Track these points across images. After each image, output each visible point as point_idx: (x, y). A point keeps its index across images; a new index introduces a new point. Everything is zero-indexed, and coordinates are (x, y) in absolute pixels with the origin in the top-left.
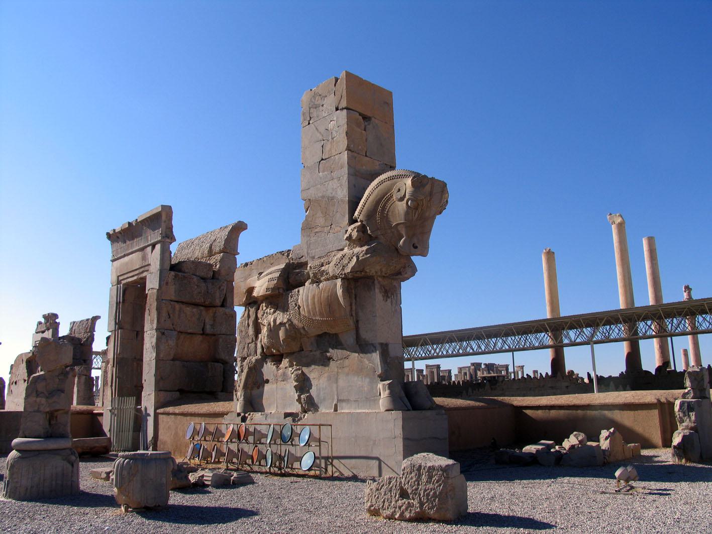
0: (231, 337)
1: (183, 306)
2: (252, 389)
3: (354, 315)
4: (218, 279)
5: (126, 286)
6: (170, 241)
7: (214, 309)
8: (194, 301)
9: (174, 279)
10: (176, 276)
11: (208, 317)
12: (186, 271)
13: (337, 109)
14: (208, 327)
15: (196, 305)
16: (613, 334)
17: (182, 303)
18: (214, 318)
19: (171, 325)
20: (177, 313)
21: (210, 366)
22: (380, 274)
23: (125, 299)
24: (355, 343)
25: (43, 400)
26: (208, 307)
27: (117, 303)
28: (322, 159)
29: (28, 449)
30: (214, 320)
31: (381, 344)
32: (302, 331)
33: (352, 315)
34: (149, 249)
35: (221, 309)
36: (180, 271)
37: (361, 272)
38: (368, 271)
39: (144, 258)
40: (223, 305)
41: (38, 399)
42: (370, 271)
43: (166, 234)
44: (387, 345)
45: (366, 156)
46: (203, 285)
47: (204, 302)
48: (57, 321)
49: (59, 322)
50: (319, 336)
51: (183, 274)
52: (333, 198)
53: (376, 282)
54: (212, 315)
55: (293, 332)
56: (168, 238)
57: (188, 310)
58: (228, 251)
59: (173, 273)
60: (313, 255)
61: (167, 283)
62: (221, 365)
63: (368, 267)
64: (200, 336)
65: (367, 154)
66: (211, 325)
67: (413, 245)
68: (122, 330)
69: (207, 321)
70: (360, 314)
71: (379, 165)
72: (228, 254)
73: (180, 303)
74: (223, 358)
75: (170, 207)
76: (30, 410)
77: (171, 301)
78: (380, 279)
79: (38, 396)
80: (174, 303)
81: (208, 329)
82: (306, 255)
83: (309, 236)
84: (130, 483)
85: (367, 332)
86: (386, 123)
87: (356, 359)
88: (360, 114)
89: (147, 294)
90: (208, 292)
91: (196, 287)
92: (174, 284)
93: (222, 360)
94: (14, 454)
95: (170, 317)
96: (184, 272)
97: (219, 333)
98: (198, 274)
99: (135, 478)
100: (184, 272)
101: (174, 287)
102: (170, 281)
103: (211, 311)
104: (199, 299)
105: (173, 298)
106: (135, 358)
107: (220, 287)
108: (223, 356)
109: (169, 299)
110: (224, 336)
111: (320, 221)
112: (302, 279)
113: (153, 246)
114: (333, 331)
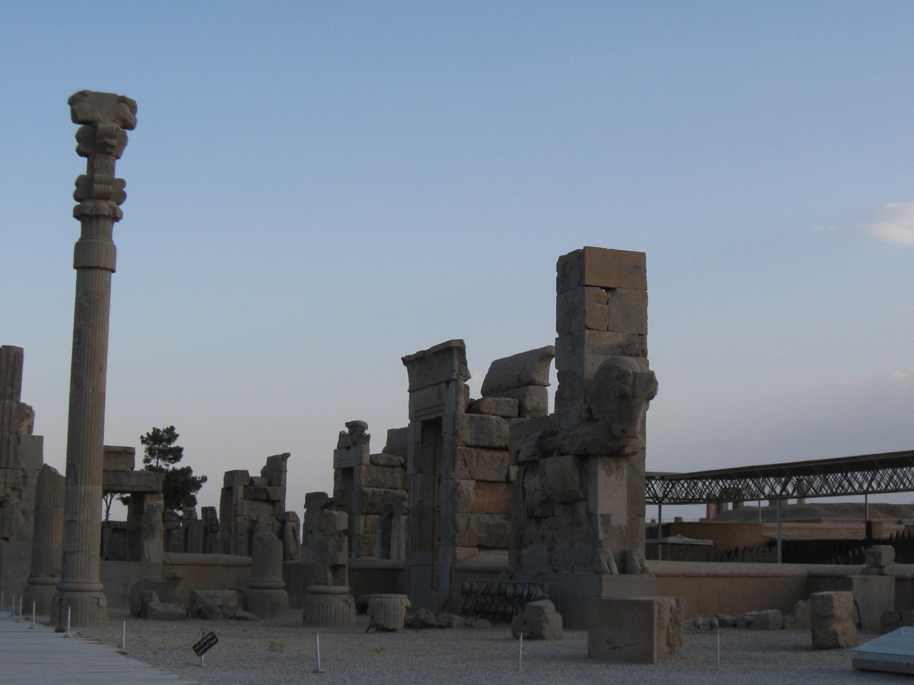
9: (469, 423)
10: (472, 419)
12: (485, 411)
27: (415, 443)
28: (570, 333)
34: (444, 385)
36: (478, 411)
44: (609, 516)
48: (367, 432)
49: (369, 435)
51: (479, 415)
65: (609, 329)
71: (624, 336)
80: (470, 449)
86: (636, 289)
92: (470, 428)
95: (466, 464)
96: (483, 413)
98: (499, 413)
100: (483, 413)
102: (465, 425)
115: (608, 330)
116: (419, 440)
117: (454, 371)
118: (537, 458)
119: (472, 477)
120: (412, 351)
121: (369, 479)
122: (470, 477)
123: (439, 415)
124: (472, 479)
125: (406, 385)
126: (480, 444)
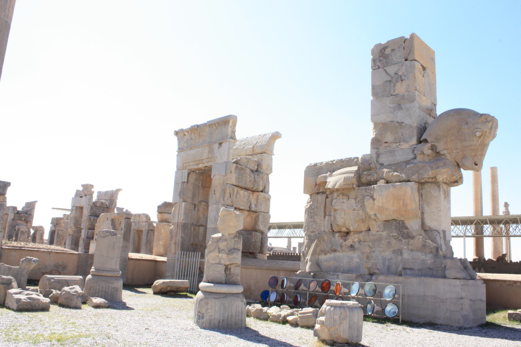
0: (267, 214)
1: (239, 189)
2: (319, 255)
3: (421, 208)
4: (260, 172)
5: (190, 171)
6: (233, 141)
7: (257, 193)
8: (247, 186)
10: (237, 167)
11: (253, 198)
12: (242, 164)
14: (253, 206)
15: (246, 189)
16: (487, 231)
17: (238, 187)
18: (257, 199)
19: (231, 203)
20: (235, 194)
21: (254, 235)
22: (445, 181)
23: (189, 180)
24: (421, 228)
25: (224, 256)
26: (253, 191)
29: (218, 292)
30: (257, 202)
31: (443, 231)
32: (373, 217)
33: (420, 209)
34: (216, 146)
35: (262, 194)
37: (432, 178)
38: (438, 178)
39: (211, 151)
40: (262, 191)
41: (220, 255)
42: (439, 178)
43: (231, 136)
45: (424, 96)
46: (252, 175)
47: (253, 188)
50: (386, 221)
52: (401, 123)
53: (441, 186)
54: (256, 197)
55: (364, 217)
56: (233, 139)
57: (242, 192)
58: (268, 152)
60: (382, 162)
61: (231, 172)
62: (260, 234)
63: (439, 176)
64: (247, 212)
66: (255, 205)
67: (475, 163)
68: (185, 203)
69: (252, 201)
70: (426, 208)
72: (268, 155)
73: (237, 187)
74: (261, 229)
75: (236, 117)
76: (213, 263)
77: (233, 185)
78: (443, 184)
79: (219, 252)
81: (253, 208)
82: (375, 162)
83: (377, 148)
84: (341, 325)
85: (431, 221)
87: (421, 240)
89: (212, 179)
90: (255, 181)
91: (248, 176)
93: (260, 230)
94: (200, 294)
97: (259, 211)
99: (344, 322)
100: (242, 165)
101: (235, 174)
102: (233, 170)
103: (255, 195)
104: (250, 186)
105: (234, 183)
106: (193, 224)
107: (262, 178)
108: (261, 227)
109: (231, 183)
110: (263, 213)
111: (389, 137)
112: (372, 179)
113: (220, 144)
114: (402, 219)
116: (186, 181)
117: (228, 136)
118: (355, 186)
119: (232, 205)
120: (186, 126)
121: (92, 212)
122: (231, 205)
123: (209, 164)
124: (233, 206)
125: (176, 147)
126: (240, 185)
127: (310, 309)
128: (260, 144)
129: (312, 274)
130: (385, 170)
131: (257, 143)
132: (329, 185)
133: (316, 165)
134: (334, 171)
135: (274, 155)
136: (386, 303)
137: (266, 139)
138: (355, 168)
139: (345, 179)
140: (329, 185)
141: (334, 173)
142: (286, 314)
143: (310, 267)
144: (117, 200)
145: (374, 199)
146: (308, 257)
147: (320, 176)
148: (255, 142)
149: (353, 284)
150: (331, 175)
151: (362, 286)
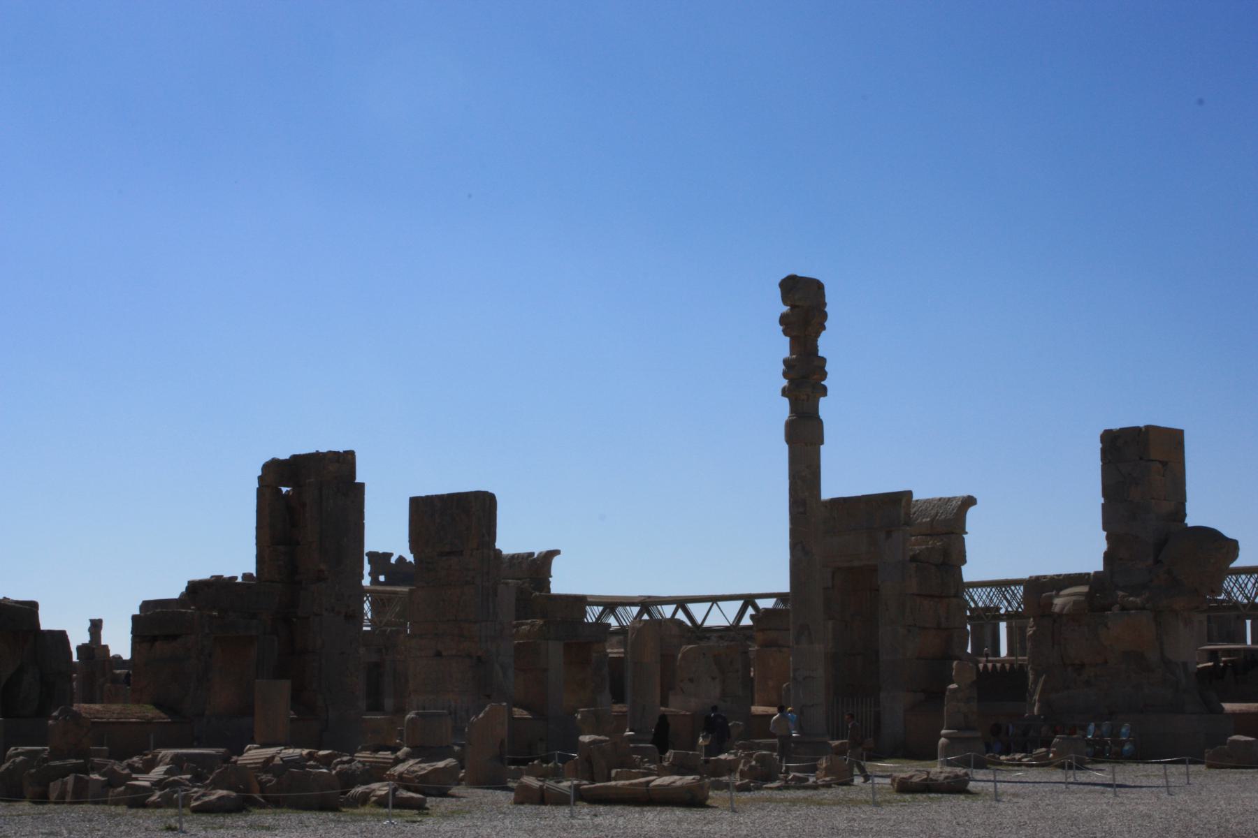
13: (1141, 459)
59: (914, 565)
88: (1160, 462)
113: (889, 534)
115: (1165, 500)
127: (1044, 749)
128: (943, 517)
129: (1042, 717)
130: (1120, 593)
131: (937, 515)
132: (1056, 609)
133: (1038, 578)
134: (1061, 590)
135: (966, 533)
136: (1122, 744)
137: (953, 510)
138: (1085, 589)
139: (1075, 603)
140: (1056, 609)
141: (1063, 592)
142: (1020, 757)
143: (1040, 709)
144: (551, 579)
145: (1108, 629)
146: (1036, 697)
147: (1044, 595)
148: (933, 512)
149: (1089, 725)
150: (1057, 595)
151: (1098, 727)
